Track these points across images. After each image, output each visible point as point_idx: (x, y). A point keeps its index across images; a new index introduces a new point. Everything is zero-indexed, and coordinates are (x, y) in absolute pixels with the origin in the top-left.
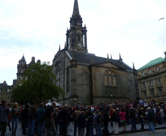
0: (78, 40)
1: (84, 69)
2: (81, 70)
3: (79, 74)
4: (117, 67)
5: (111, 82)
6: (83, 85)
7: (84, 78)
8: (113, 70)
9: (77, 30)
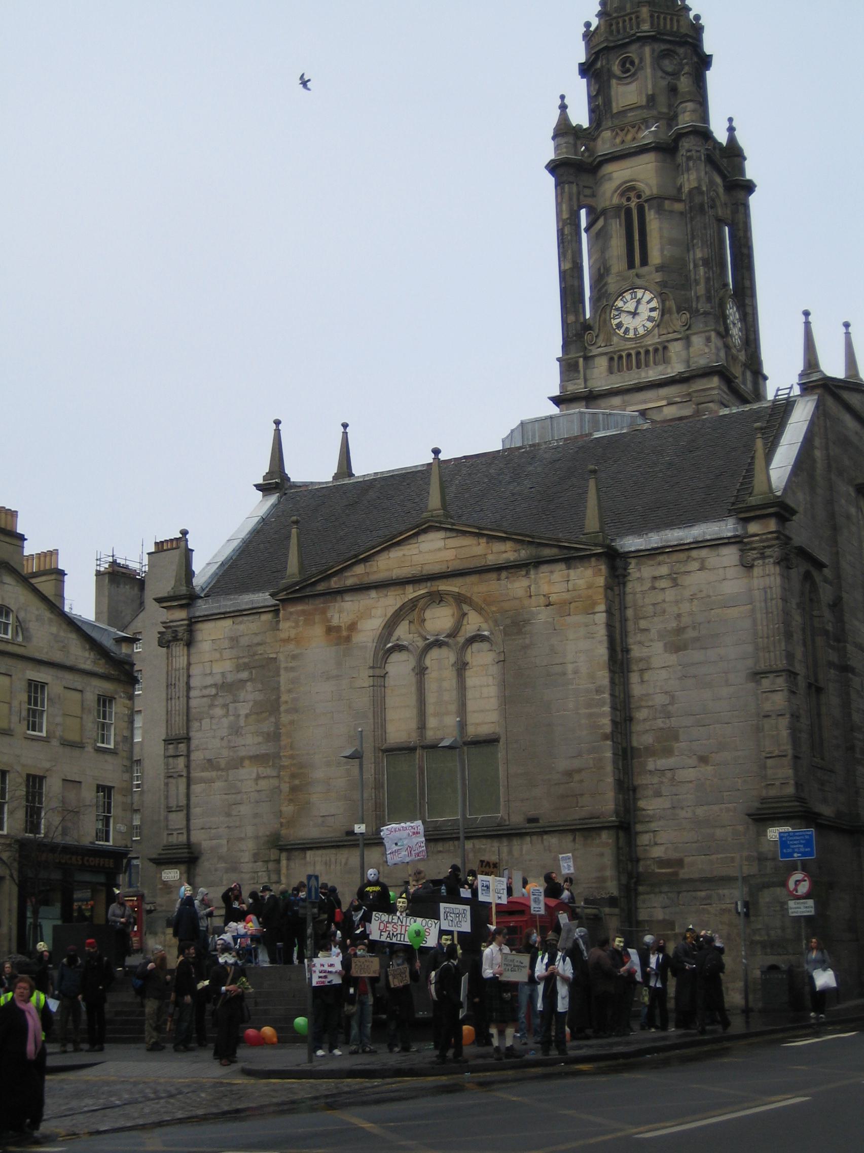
0: (631, 265)
1: (244, 641)
2: (227, 654)
4: (505, 552)
5: (450, 696)
6: (237, 763)
7: (244, 709)
8: (463, 591)
9: (609, 168)
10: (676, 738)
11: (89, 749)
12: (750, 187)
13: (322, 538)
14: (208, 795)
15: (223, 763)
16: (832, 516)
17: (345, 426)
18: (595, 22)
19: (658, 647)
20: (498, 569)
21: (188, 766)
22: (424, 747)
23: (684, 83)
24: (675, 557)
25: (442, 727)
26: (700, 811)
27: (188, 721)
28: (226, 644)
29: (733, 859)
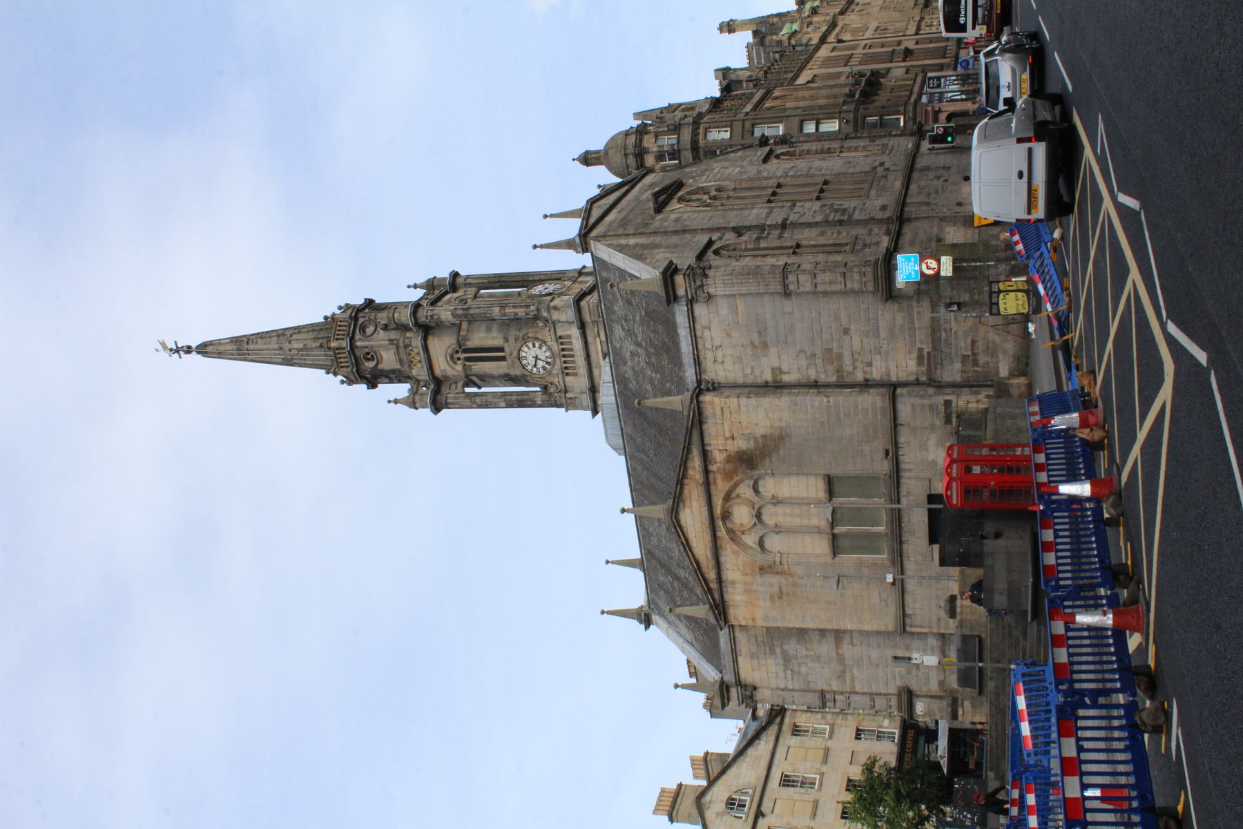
0: (503, 359)
2: (763, 662)
3: (789, 676)
6: (841, 659)
7: (804, 652)
8: (722, 496)
9: (438, 372)
10: (830, 350)
11: (829, 744)
12: (455, 275)
13: (685, 587)
14: (862, 680)
15: (840, 668)
16: (676, 232)
17: (608, 562)
18: (340, 378)
19: (764, 361)
20: (706, 472)
21: (842, 693)
22: (833, 528)
23: (383, 317)
24: (700, 347)
25: (820, 517)
26: (883, 335)
27: (809, 691)
28: (755, 661)
29: (919, 313)
